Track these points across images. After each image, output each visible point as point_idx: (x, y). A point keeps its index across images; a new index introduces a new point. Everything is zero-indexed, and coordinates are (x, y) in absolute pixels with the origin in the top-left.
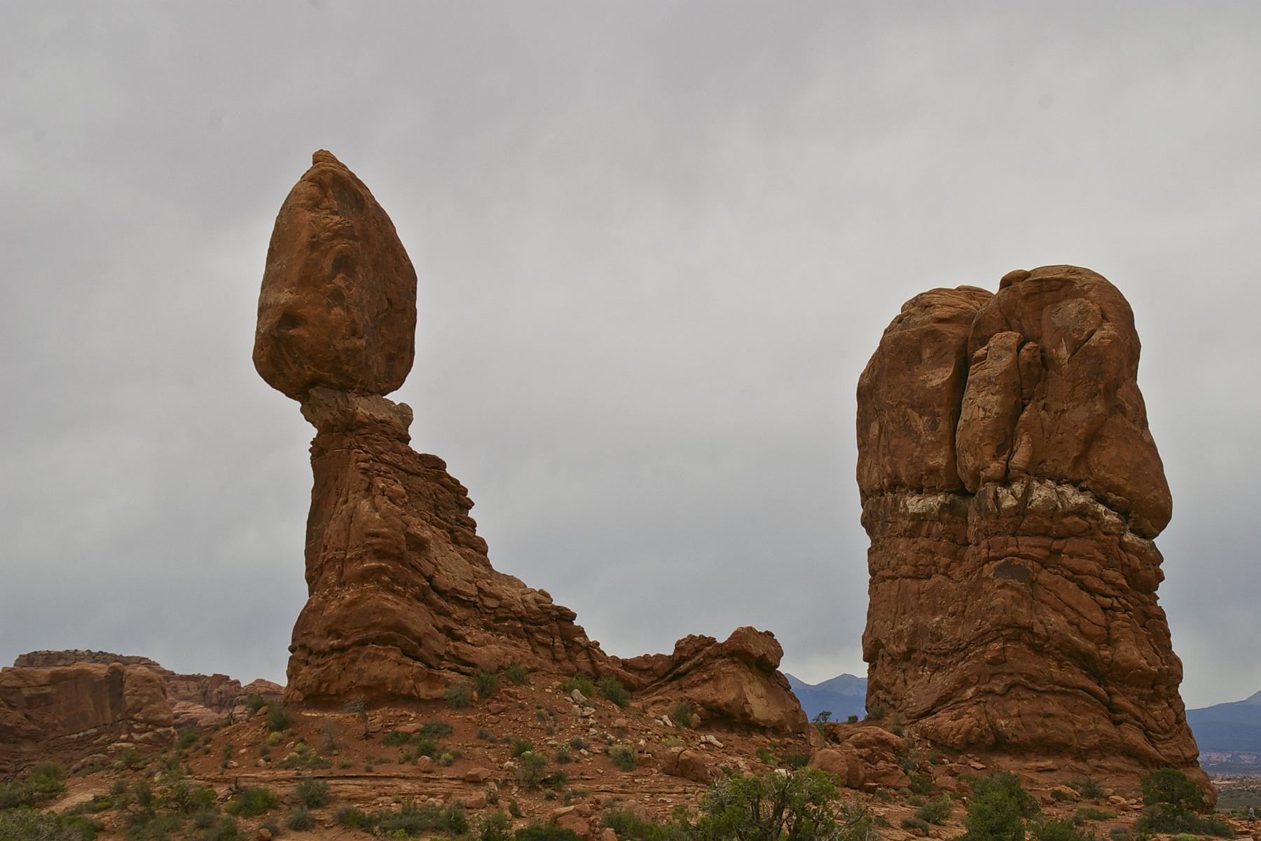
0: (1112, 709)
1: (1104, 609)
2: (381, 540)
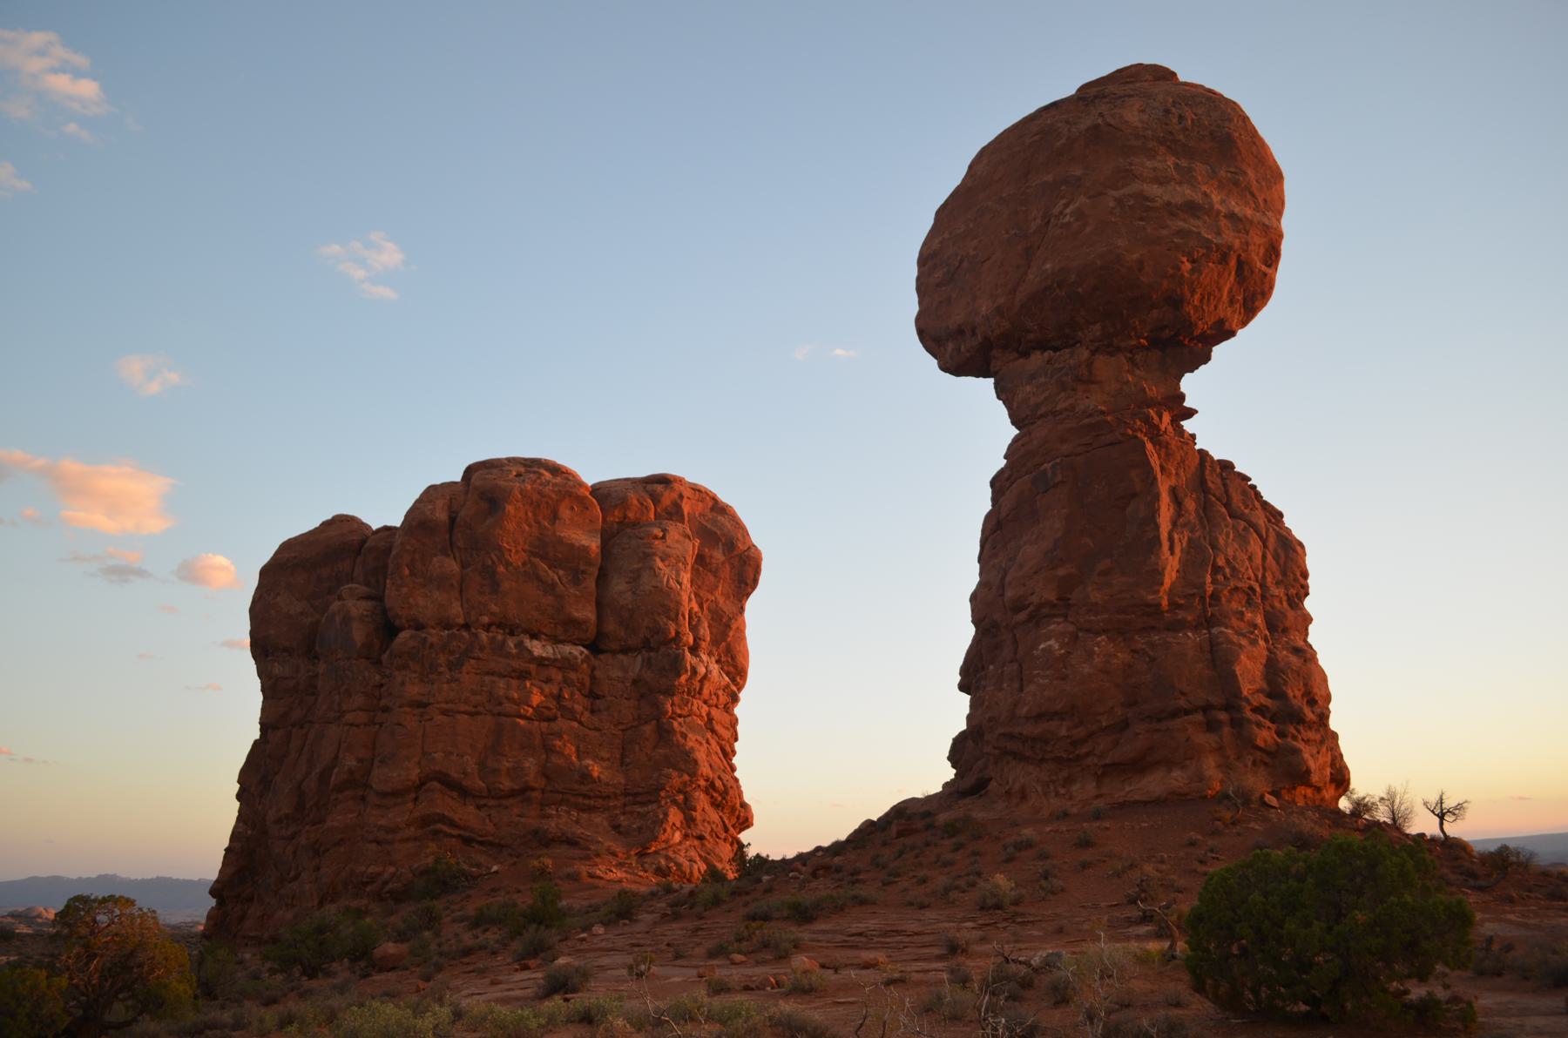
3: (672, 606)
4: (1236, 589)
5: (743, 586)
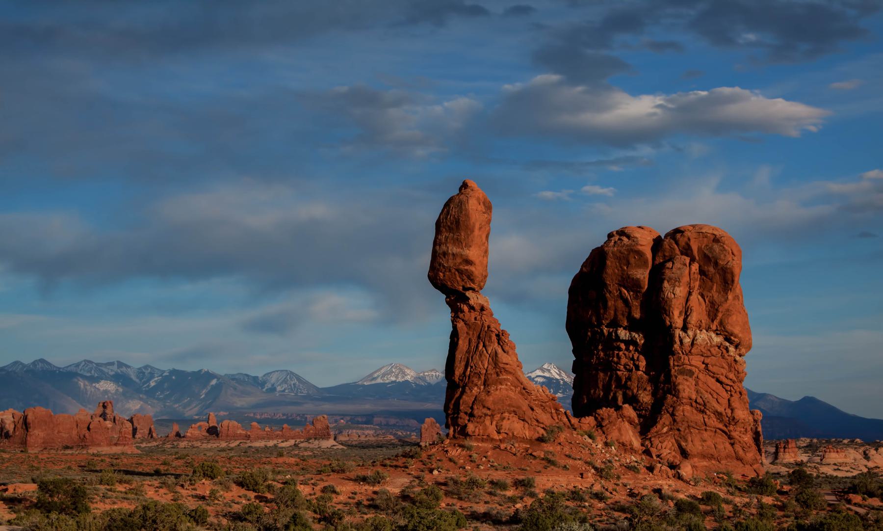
0: (730, 437)
1: (726, 391)
2: (508, 366)
3: (667, 308)
4: (475, 373)
5: (727, 285)
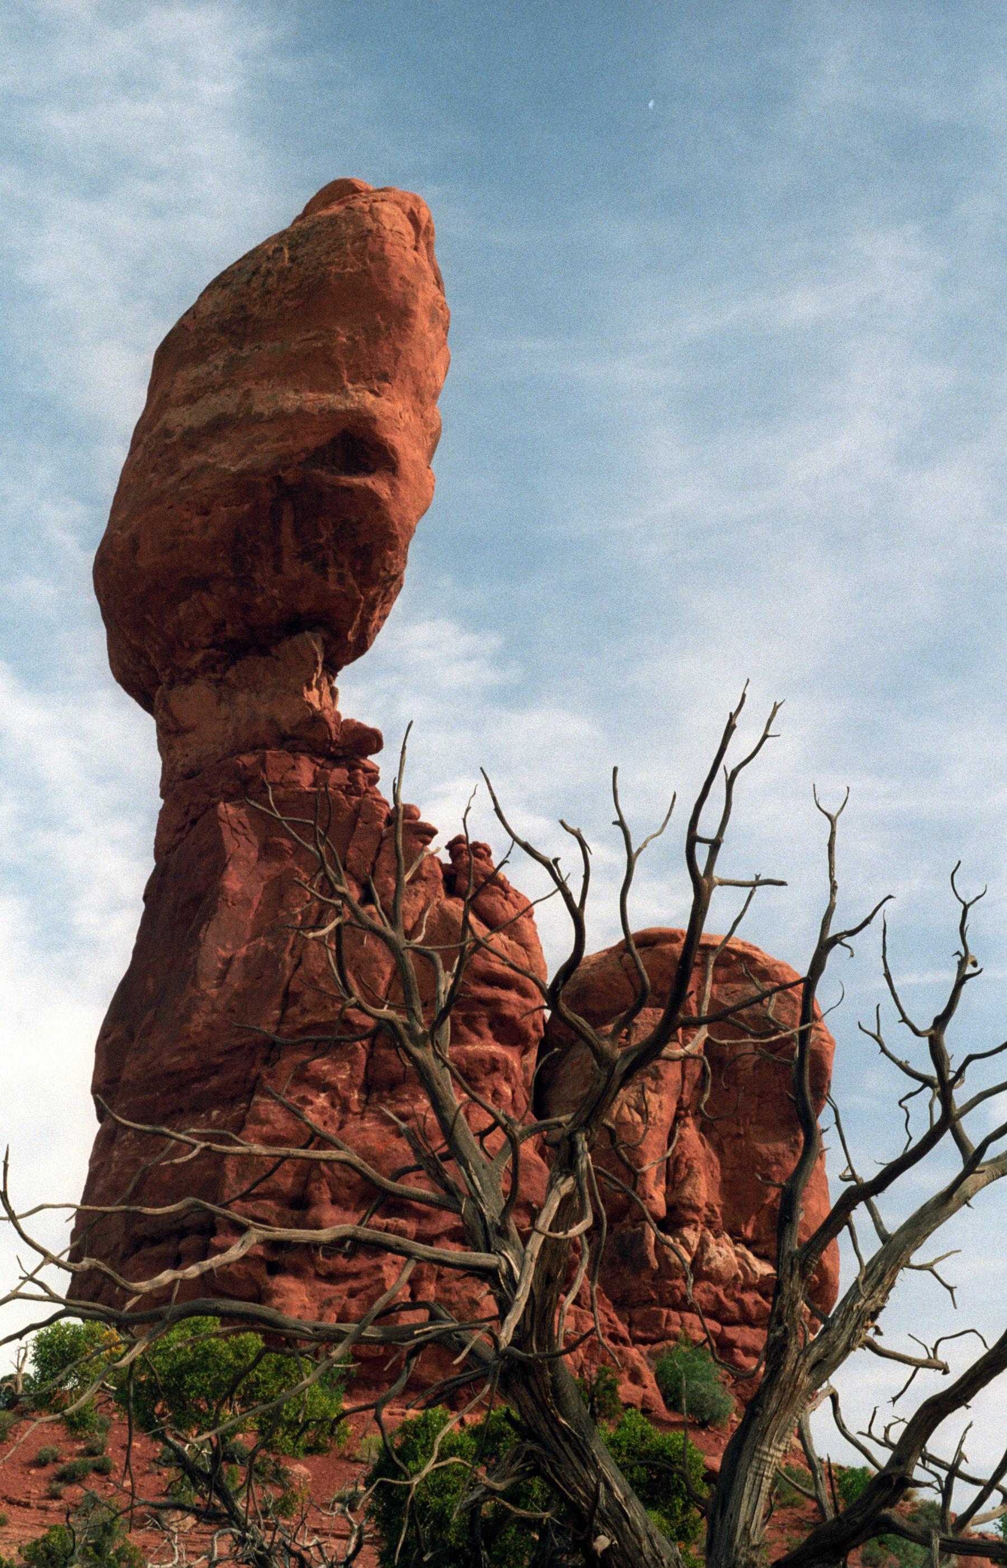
2: (513, 996)
